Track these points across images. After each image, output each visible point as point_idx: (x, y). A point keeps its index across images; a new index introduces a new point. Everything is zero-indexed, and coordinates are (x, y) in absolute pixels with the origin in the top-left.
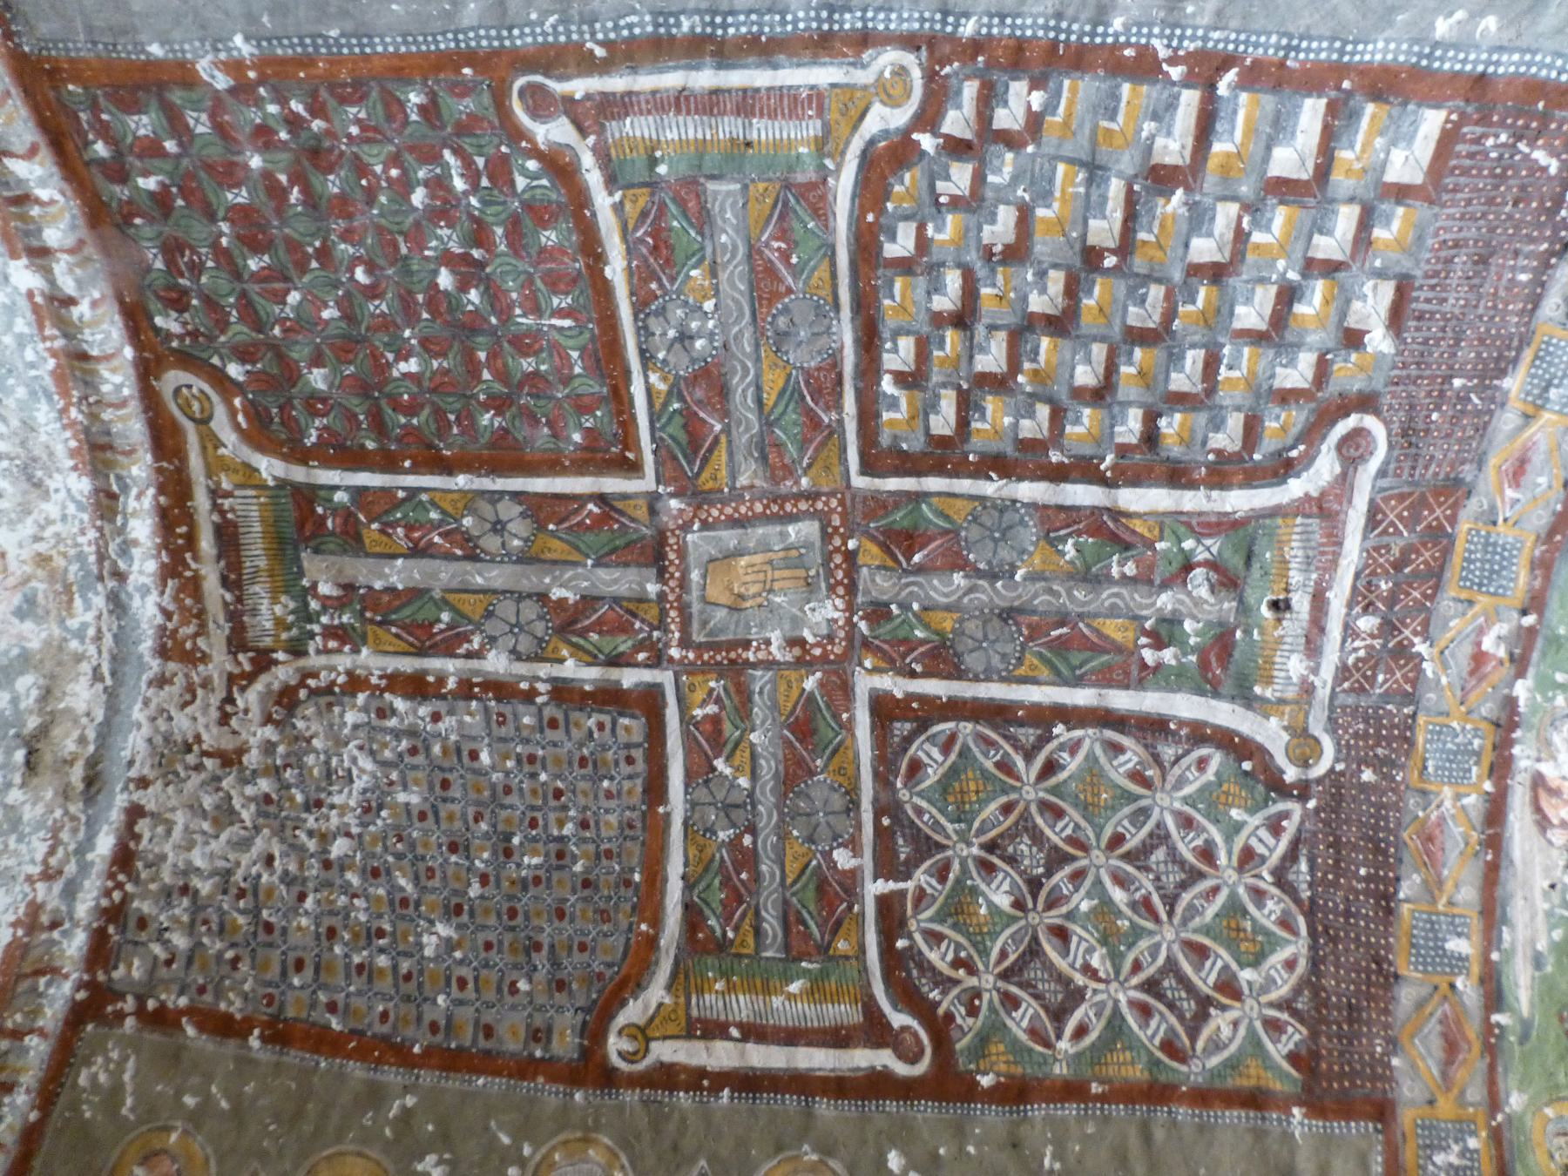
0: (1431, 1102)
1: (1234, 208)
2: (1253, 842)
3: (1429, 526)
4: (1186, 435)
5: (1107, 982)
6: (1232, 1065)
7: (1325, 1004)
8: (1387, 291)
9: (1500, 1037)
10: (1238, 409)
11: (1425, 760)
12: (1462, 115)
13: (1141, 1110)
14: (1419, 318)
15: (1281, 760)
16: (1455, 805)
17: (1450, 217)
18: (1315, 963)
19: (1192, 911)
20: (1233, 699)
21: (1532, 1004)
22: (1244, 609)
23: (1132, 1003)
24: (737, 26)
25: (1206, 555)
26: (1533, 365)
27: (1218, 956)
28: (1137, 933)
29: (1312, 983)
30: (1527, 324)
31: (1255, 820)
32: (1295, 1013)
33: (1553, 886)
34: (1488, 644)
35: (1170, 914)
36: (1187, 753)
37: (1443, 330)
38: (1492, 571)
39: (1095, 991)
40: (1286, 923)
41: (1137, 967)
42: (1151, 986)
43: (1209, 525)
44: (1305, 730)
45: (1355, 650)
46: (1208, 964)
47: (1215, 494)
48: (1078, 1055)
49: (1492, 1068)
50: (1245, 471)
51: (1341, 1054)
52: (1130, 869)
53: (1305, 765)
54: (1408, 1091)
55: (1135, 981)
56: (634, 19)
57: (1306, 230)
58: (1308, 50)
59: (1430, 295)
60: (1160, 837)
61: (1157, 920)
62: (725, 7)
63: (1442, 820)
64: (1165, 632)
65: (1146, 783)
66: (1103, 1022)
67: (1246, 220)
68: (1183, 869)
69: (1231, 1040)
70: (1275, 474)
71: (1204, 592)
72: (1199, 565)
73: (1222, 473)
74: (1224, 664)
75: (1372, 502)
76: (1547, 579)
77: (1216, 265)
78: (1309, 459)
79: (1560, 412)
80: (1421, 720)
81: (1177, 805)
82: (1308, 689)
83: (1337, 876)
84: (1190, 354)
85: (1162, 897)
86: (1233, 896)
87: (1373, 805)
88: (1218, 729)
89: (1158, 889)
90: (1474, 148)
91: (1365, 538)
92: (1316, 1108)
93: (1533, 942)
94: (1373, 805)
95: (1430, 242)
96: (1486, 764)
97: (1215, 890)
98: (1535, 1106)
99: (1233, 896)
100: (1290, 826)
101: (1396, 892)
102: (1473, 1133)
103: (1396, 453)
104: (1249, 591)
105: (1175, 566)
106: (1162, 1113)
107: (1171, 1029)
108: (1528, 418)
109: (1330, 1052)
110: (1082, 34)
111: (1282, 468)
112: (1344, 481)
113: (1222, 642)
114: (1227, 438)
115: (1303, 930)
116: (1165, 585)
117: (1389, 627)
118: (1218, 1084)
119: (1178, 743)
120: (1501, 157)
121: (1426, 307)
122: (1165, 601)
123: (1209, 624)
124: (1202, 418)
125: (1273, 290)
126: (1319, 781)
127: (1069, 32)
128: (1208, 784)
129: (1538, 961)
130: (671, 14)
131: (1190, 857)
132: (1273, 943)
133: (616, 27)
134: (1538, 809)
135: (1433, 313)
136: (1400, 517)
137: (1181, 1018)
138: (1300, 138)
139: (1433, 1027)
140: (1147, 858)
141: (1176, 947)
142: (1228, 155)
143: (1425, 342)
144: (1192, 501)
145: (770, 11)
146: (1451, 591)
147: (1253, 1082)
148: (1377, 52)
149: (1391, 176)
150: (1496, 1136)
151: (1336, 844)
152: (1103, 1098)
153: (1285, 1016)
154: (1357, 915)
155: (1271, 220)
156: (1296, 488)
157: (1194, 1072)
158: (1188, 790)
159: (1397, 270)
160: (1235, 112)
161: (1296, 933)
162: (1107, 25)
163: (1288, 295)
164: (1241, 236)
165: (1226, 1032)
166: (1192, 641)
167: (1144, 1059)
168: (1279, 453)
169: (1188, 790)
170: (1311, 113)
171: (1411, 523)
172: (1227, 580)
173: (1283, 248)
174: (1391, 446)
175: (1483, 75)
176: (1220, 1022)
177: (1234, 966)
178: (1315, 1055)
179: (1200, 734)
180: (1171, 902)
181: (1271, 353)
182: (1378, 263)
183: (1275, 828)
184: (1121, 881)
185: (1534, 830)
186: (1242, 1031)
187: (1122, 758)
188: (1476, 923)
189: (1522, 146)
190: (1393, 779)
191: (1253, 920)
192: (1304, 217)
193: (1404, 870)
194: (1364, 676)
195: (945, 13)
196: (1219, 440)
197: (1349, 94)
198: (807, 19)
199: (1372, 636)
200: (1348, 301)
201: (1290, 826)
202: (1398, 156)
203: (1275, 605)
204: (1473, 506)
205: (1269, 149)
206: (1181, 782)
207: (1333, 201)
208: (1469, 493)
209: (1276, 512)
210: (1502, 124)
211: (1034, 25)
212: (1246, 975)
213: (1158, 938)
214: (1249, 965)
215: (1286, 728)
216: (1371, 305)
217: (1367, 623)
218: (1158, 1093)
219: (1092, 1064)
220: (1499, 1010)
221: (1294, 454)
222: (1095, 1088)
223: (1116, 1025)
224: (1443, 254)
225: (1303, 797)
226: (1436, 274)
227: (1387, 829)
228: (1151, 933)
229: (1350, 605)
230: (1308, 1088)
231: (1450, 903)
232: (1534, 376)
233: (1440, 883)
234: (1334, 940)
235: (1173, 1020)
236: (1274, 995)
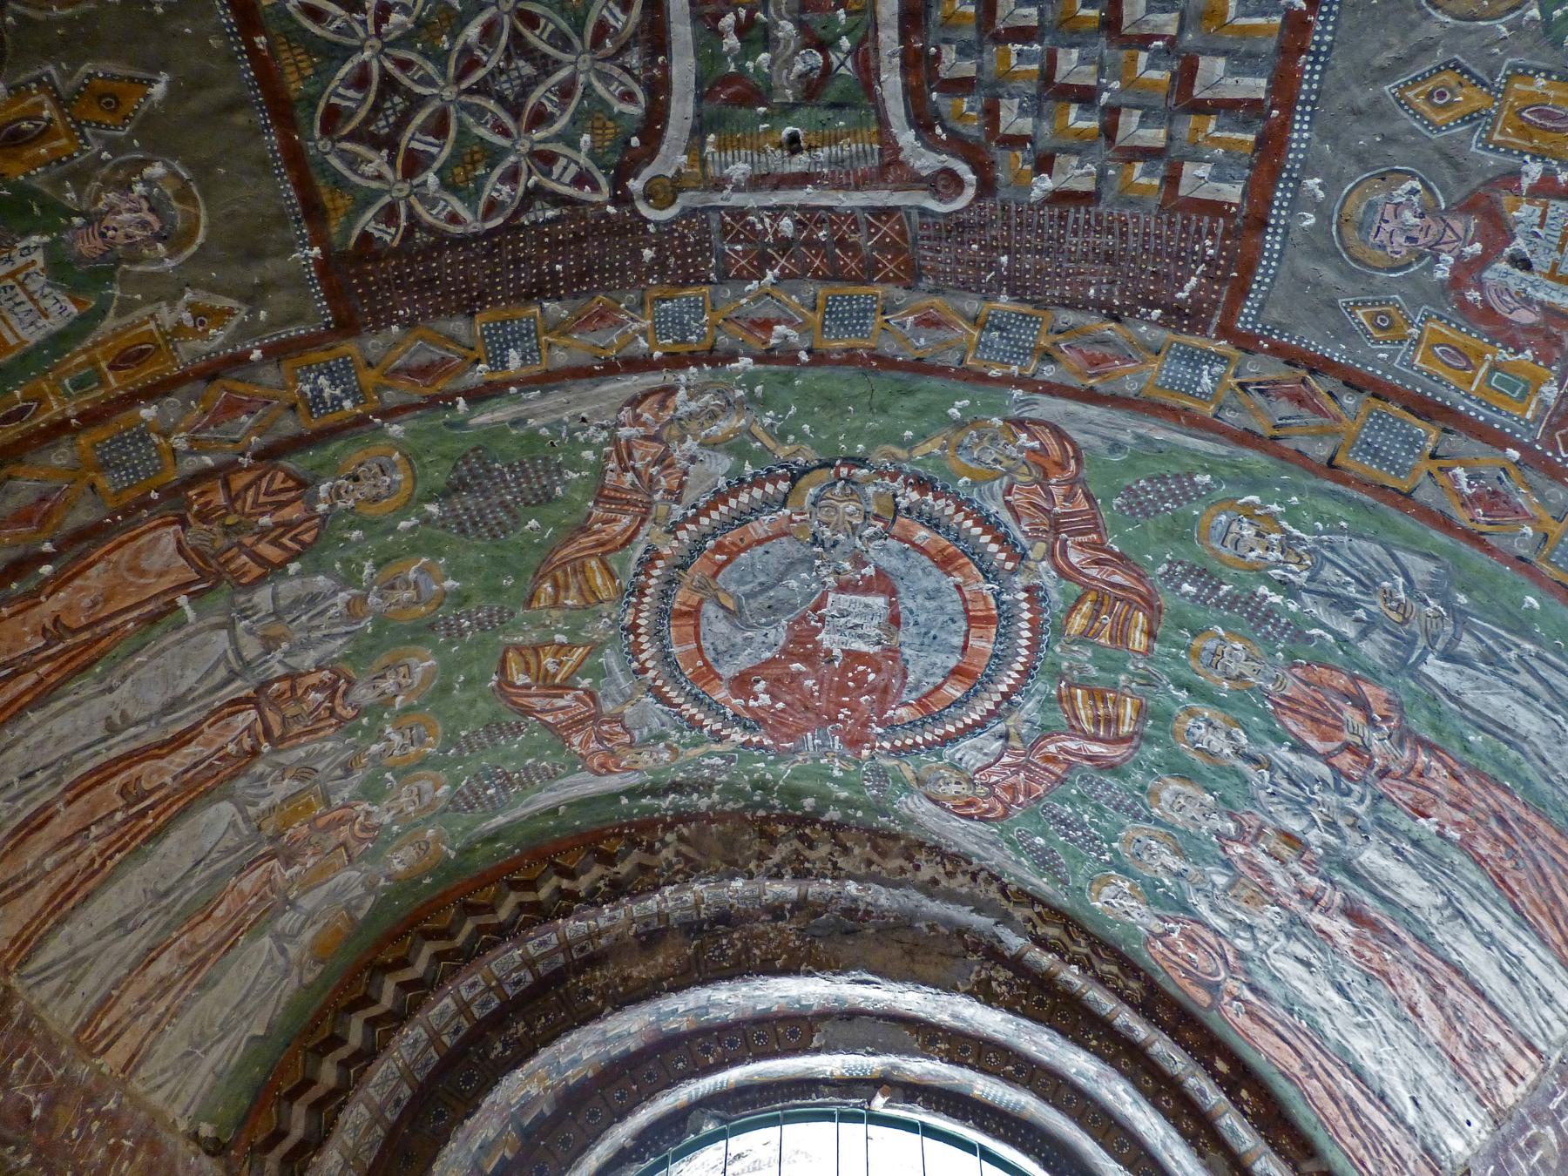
0: (369, 364)
1: (1172, 30)
2: (562, 162)
3: (878, 261)
4: (953, 21)
5: (378, 34)
6: (339, 182)
7: (428, 258)
8: (1087, 185)
9: (446, 407)
10: (980, 68)
11: (671, 300)
12: (1235, 215)
13: (258, 96)
14: (1061, 217)
15: (647, 173)
16: (638, 332)
17: (1147, 224)
18: (463, 241)
19: (479, 113)
20: (698, 115)
21: (480, 426)
22: (787, 110)
23: (364, 66)
25: (836, 63)
26: (1018, 314)
27: (441, 147)
28: (440, 59)
29: (442, 242)
30: (1053, 303)
31: (583, 160)
32: (409, 232)
33: (584, 420)
34: (780, 329)
35: (469, 91)
36: (636, 79)
37: (1051, 238)
38: (842, 320)
39: (364, 23)
40: (493, 207)
41: (405, 65)
42: (389, 85)
43: (866, 60)
44: (681, 190)
45: (762, 221)
46: (430, 139)
47: (897, 60)
48: (289, 15)
49: (418, 406)
50: (920, 87)
51: (386, 281)
52: (504, 39)
53: (647, 196)
54: (373, 344)
55: (388, 65)
57: (1146, 102)
58: (1312, 72)
59: (1081, 222)
60: (546, 66)
61: (459, 78)
63: (621, 324)
64: (755, 35)
65: (597, 42)
66: (335, 38)
67: (1160, 43)
68: (517, 96)
69: (362, 175)
70: (918, 116)
71: (799, 67)
72: (826, 58)
73: (917, 64)
74: (730, 99)
75: (898, 208)
76: (839, 363)
77: (1120, 20)
78: (933, 145)
79: (979, 342)
80: (706, 289)
81: (582, 78)
82: (718, 185)
83: (548, 246)
84: (1033, 11)
85: (484, 79)
86: (503, 152)
87: (622, 263)
88: (666, 105)
89: (491, 73)
90: (1204, 231)
91: (864, 209)
92: (325, 267)
93: (533, 416)
94: (622, 263)
95: (1127, 212)
96: (676, 349)
97: (506, 133)
98: (397, 444)
99: (503, 152)
100: (586, 193)
101: (547, 299)
102: (356, 403)
103: (941, 221)
104: (804, 111)
105: (820, 32)
106: (263, 118)
107: (352, 114)
108: (974, 320)
109: (384, 271)
111: (922, 121)
112: (914, 181)
113: (752, 93)
114: (952, 63)
115: (490, 225)
116: (801, 26)
117: (784, 245)
118: (314, 171)
119: (646, 69)
120: (1195, 253)
121: (1071, 220)
122: (787, 28)
123: (768, 77)
124: (970, 35)
125: (1092, 82)
126: (635, 212)
128: (608, 106)
129: (517, 422)
131: (532, 101)
132: (470, 199)
134: (646, 396)
135: (1064, 228)
136: (886, 235)
137: (367, 121)
138: (1231, 81)
139: (437, 353)
140: (520, 57)
141: (437, 103)
142: (1224, 15)
143: (1040, 226)
144: (889, 38)
146: (822, 291)
147: (329, 205)
148: (1301, 132)
149: (1187, 167)
150: (361, 421)
151: (578, 239)
152: (253, 51)
153: (403, 223)
154: (517, 270)
155: (1158, 68)
156: (907, 138)
157: (318, 144)
158: (599, 87)
159: (1105, 190)
160: (1264, 14)
161: (486, 218)
163: (1085, 97)
164: (1144, 41)
165: (369, 169)
166: (749, 64)
167: (311, 90)
168: (938, 116)
169: (599, 87)
170: (1255, 86)
171: (881, 246)
172: (813, 88)
173: (1132, 84)
174: (946, 215)
175: (1267, 225)
176: (376, 162)
177: (436, 165)
178: (376, 257)
179: (658, 88)
180: (482, 89)
181: (1033, 91)
182: (1111, 172)
183: (581, 180)
184: (489, 31)
185: (628, 396)
186: (375, 185)
187: (617, 11)
188: (536, 369)
189: (1202, 267)
190: (648, 277)
191: (487, 176)
192: (1159, 100)
193: (568, 301)
194: (739, 232)
196: (949, 55)
197: (1267, 117)
199: (776, 232)
200: (1078, 153)
201: (586, 193)
202: (1204, 171)
203: (794, 138)
204: (898, 293)
205: (1225, 53)
206: (606, 78)
207: (1171, 121)
208: (908, 288)
209: (883, 123)
210: (1223, 248)
212: (431, 178)
213: (441, 83)
214: (441, 180)
215: (678, 171)
216: (1075, 174)
217: (786, 225)
218: (283, 112)
219: (285, 33)
220: (468, 402)
221: (939, 130)
222: (261, 41)
223: (336, 53)
224: (1116, 225)
225: (615, 200)
226: (1099, 223)
227: (604, 279)
228: (444, 74)
229: (802, 208)
230: (344, 256)
231: (549, 345)
232: (1009, 317)
233: (565, 334)
234: (489, 254)
235: (362, 113)
236: (420, 209)
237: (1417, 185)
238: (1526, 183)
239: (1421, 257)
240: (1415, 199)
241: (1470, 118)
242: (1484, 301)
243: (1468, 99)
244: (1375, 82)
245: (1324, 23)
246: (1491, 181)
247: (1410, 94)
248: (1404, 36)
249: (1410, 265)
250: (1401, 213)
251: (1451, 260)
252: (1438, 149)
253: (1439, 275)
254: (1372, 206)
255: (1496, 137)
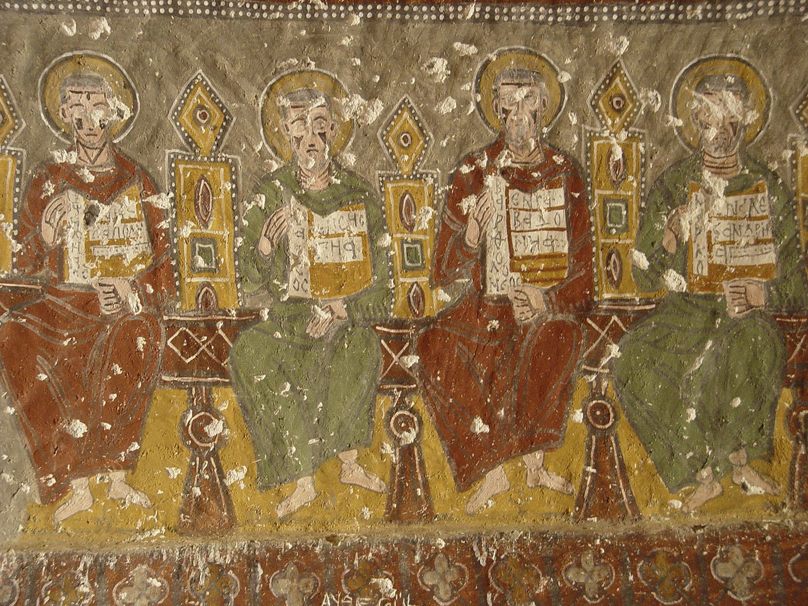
24: (657, 11)
56: (740, 16)
62: (665, 27)
110: (383, 10)
127: (393, 11)
130: (709, 21)
133: (756, 9)
145: (631, 23)
162: (364, 19)
195: (492, 20)
198: (601, 14)
211: (422, 15)
237: (127, 114)
238: (153, 199)
239: (67, 136)
240: (115, 117)
241: (190, 142)
242: (48, 199)
243: (205, 136)
244: (204, 60)
245: (244, 8)
246: (147, 174)
247: (199, 91)
248: (242, 75)
249: (58, 129)
250: (100, 108)
251: (73, 161)
252: (160, 124)
253: (56, 154)
254: (98, 81)
255: (181, 167)
